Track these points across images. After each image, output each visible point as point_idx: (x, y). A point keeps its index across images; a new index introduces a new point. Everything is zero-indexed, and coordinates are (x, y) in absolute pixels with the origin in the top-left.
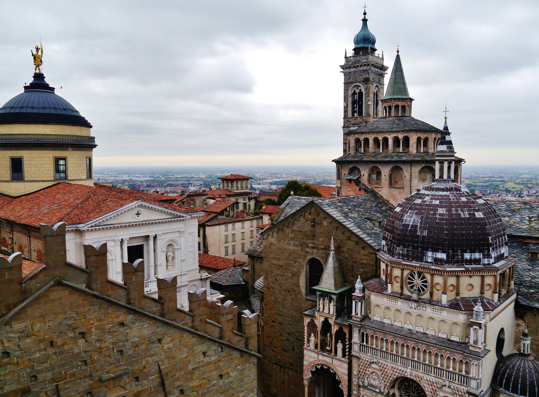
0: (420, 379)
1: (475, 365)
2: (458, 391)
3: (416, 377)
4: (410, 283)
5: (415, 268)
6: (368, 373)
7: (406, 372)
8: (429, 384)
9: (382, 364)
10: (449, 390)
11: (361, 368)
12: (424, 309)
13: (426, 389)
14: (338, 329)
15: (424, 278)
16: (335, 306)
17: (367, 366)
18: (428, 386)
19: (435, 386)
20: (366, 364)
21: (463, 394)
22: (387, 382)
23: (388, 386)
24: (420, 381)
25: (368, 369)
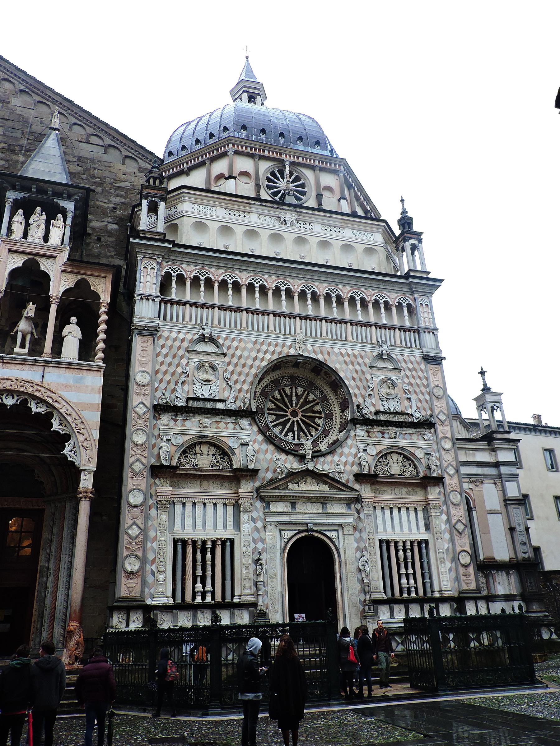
0: (326, 357)
1: (424, 305)
2: (405, 361)
3: (315, 352)
4: (269, 187)
5: (286, 155)
6: (186, 369)
7: (290, 347)
8: (346, 363)
9: (226, 339)
11: (162, 363)
12: (307, 226)
13: (342, 374)
14: (72, 285)
15: (297, 179)
16: (68, 229)
17: (181, 352)
18: (344, 365)
20: (179, 348)
21: (416, 366)
22: (244, 382)
23: (247, 392)
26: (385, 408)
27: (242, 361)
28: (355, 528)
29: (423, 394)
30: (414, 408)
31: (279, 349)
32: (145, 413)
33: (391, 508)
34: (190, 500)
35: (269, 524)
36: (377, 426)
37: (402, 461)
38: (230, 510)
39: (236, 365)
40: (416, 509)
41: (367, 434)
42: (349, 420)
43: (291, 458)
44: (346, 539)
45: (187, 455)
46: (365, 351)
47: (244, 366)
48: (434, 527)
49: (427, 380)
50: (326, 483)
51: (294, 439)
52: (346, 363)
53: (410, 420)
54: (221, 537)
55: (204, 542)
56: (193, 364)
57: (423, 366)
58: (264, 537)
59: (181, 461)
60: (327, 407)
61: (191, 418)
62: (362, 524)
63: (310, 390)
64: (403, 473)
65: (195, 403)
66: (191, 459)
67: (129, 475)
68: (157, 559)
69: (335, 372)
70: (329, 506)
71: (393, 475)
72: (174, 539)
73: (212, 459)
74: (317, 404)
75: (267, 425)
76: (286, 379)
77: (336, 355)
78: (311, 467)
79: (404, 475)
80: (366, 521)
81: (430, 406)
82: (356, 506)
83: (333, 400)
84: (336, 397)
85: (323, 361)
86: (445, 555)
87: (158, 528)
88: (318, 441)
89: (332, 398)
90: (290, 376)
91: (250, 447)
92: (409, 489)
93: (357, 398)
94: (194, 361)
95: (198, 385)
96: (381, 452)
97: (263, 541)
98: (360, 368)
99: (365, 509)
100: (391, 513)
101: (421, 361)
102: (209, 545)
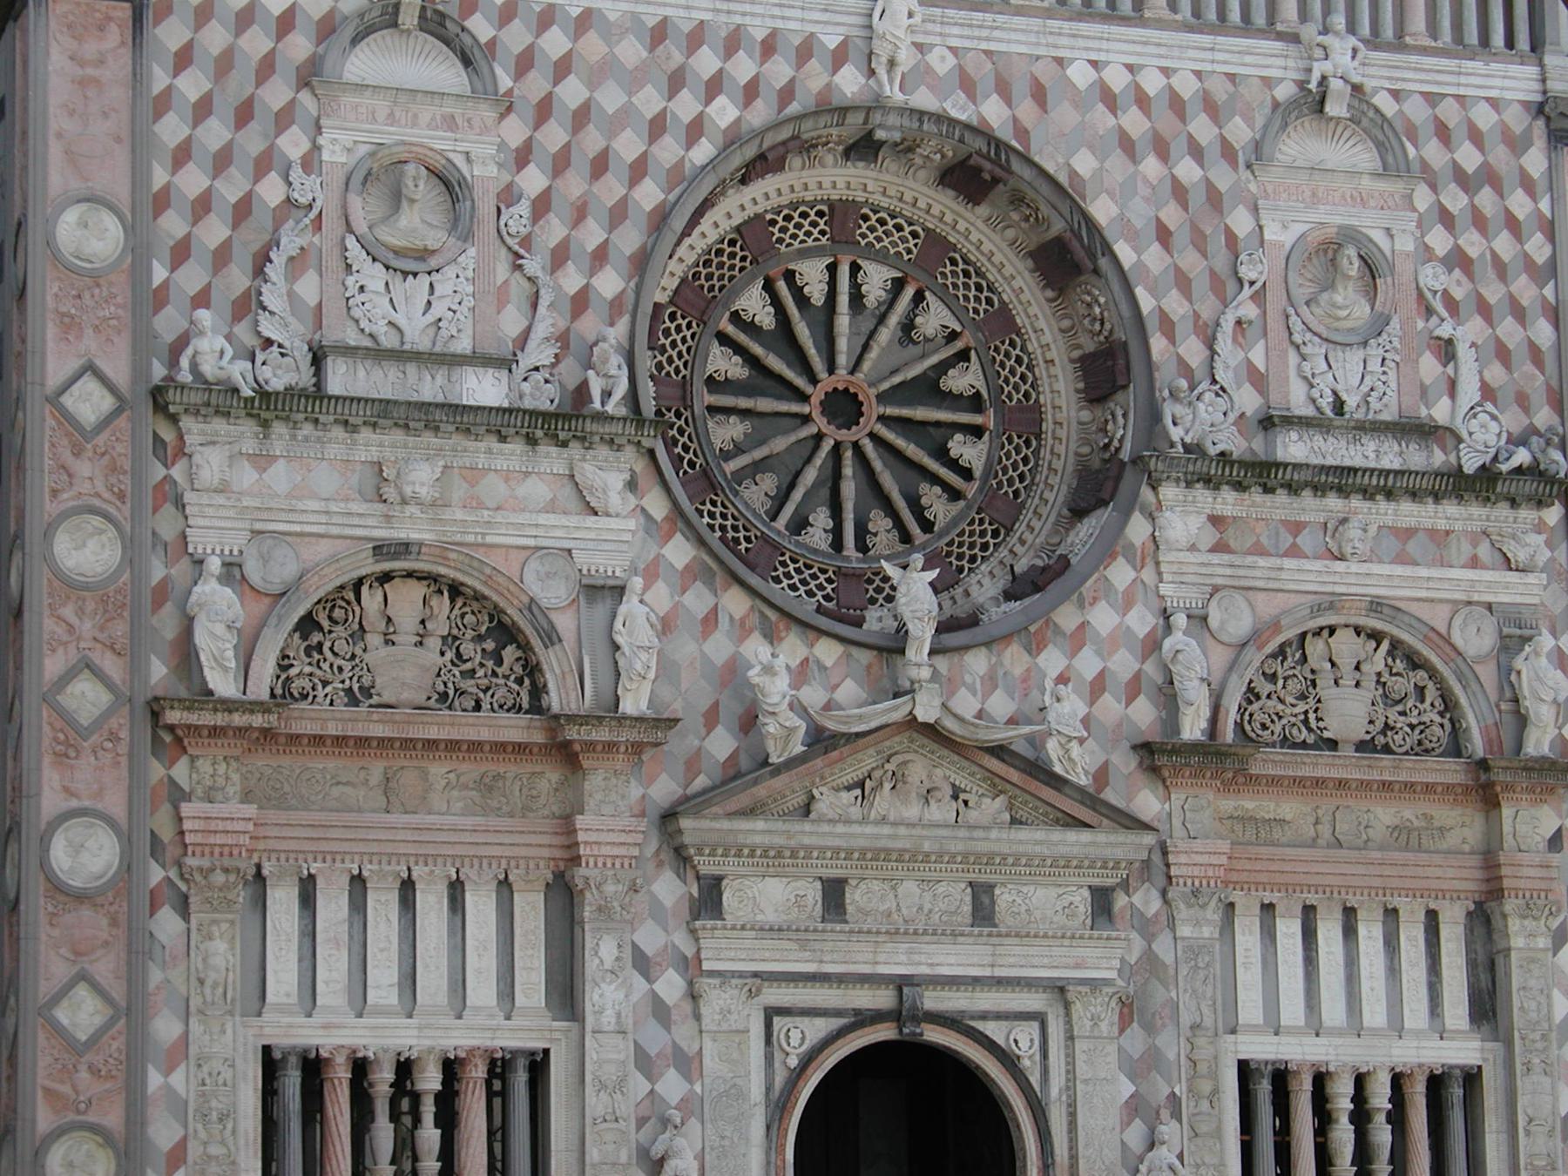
0: (1026, 110)
2: (1443, 133)
3: (968, 85)
6: (306, 188)
7: (839, 58)
8: (1127, 145)
10: (1359, 155)
11: (182, 154)
13: (1102, 210)
17: (276, 94)
18: (1117, 160)
19: (1196, 152)
20: (266, 68)
21: (1500, 156)
22: (600, 256)
24: (1022, 132)
25: (293, 144)
26: (1315, 393)
27: (592, 141)
28: (1128, 1011)
29: (1519, 313)
30: (1469, 391)
31: (780, 70)
32: (106, 422)
33: (1309, 912)
34: (338, 864)
35: (716, 981)
36: (1268, 490)
37: (1379, 674)
38: (531, 910)
39: (561, 163)
40: (1432, 917)
41: (1210, 536)
42: (1125, 455)
43: (828, 652)
44: (1080, 1058)
45: (316, 638)
46: (1232, 77)
47: (600, 166)
48: (1516, 1003)
49: (1551, 237)
50: (996, 785)
51: (838, 544)
52: (1127, 145)
53: (1438, 458)
54: (488, 1043)
55: (405, 1068)
56: (343, 160)
57: (1535, 161)
58: (690, 1047)
59: (293, 672)
60: (1012, 372)
61: (333, 450)
62: (1162, 990)
63: (925, 281)
64: (1383, 732)
65: (361, 373)
66: (339, 662)
67: (46, 742)
68: (194, 1151)
69: (1066, 195)
70: (1004, 898)
71: (1333, 744)
72: (267, 1050)
73: (440, 661)
74: (963, 356)
75: (706, 473)
76: (804, 215)
77: (1079, 101)
78: (923, 715)
79: (1387, 749)
80: (1183, 971)
81: (1554, 383)
82: (1137, 899)
83: (1047, 338)
84: (1066, 323)
85: (1006, 134)
86: (1560, 1145)
87: (195, 1002)
88: (960, 557)
89: (1042, 324)
90: (831, 205)
91: (630, 606)
92: (1408, 814)
93: (1174, 343)
94: (346, 138)
95: (374, 276)
96: (1276, 627)
97: (688, 1064)
98: (1197, 173)
99: (1182, 912)
100: (1309, 935)
101: (1529, 130)
102: (430, 1081)
